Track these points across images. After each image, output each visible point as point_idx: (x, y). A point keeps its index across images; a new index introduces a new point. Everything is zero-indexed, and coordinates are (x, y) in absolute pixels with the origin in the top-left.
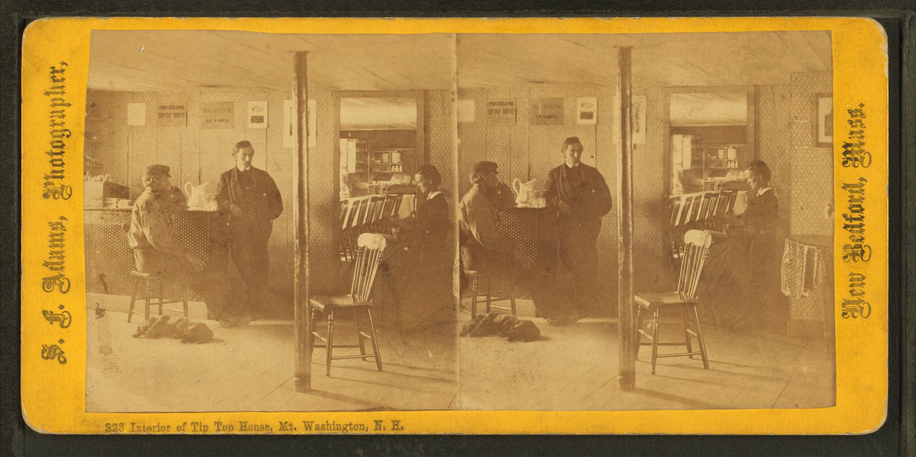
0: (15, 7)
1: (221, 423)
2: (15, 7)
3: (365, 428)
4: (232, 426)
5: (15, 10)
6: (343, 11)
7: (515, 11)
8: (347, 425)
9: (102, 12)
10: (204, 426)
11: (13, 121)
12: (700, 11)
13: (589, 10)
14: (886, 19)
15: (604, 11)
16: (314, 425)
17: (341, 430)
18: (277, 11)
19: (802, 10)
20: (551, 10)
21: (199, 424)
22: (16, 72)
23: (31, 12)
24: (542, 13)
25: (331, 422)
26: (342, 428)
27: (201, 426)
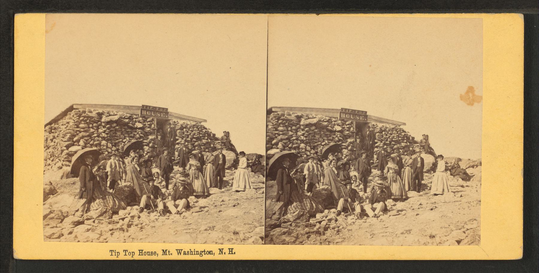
0: (11, 7)
1: (127, 250)
2: (11, 7)
3: (213, 253)
4: (134, 252)
5: (11, 8)
6: (207, 10)
7: (310, 10)
8: (202, 252)
9: (63, 10)
10: (117, 253)
11: (10, 75)
12: (421, 10)
13: (354, 9)
14: (532, 15)
15: (363, 10)
16: (183, 251)
17: (198, 254)
18: (168, 9)
19: (482, 9)
20: (331, 9)
21: (114, 251)
22: (12, 46)
23: (20, 10)
24: (327, 11)
25: (193, 250)
26: (199, 253)
27: (115, 252)
